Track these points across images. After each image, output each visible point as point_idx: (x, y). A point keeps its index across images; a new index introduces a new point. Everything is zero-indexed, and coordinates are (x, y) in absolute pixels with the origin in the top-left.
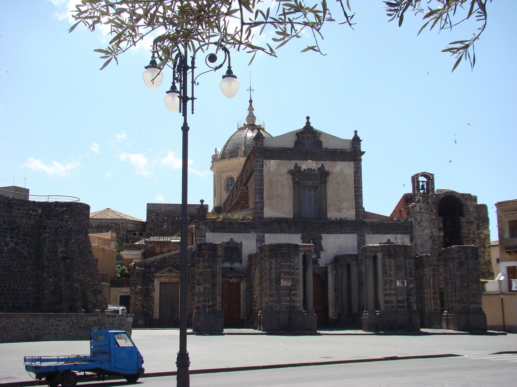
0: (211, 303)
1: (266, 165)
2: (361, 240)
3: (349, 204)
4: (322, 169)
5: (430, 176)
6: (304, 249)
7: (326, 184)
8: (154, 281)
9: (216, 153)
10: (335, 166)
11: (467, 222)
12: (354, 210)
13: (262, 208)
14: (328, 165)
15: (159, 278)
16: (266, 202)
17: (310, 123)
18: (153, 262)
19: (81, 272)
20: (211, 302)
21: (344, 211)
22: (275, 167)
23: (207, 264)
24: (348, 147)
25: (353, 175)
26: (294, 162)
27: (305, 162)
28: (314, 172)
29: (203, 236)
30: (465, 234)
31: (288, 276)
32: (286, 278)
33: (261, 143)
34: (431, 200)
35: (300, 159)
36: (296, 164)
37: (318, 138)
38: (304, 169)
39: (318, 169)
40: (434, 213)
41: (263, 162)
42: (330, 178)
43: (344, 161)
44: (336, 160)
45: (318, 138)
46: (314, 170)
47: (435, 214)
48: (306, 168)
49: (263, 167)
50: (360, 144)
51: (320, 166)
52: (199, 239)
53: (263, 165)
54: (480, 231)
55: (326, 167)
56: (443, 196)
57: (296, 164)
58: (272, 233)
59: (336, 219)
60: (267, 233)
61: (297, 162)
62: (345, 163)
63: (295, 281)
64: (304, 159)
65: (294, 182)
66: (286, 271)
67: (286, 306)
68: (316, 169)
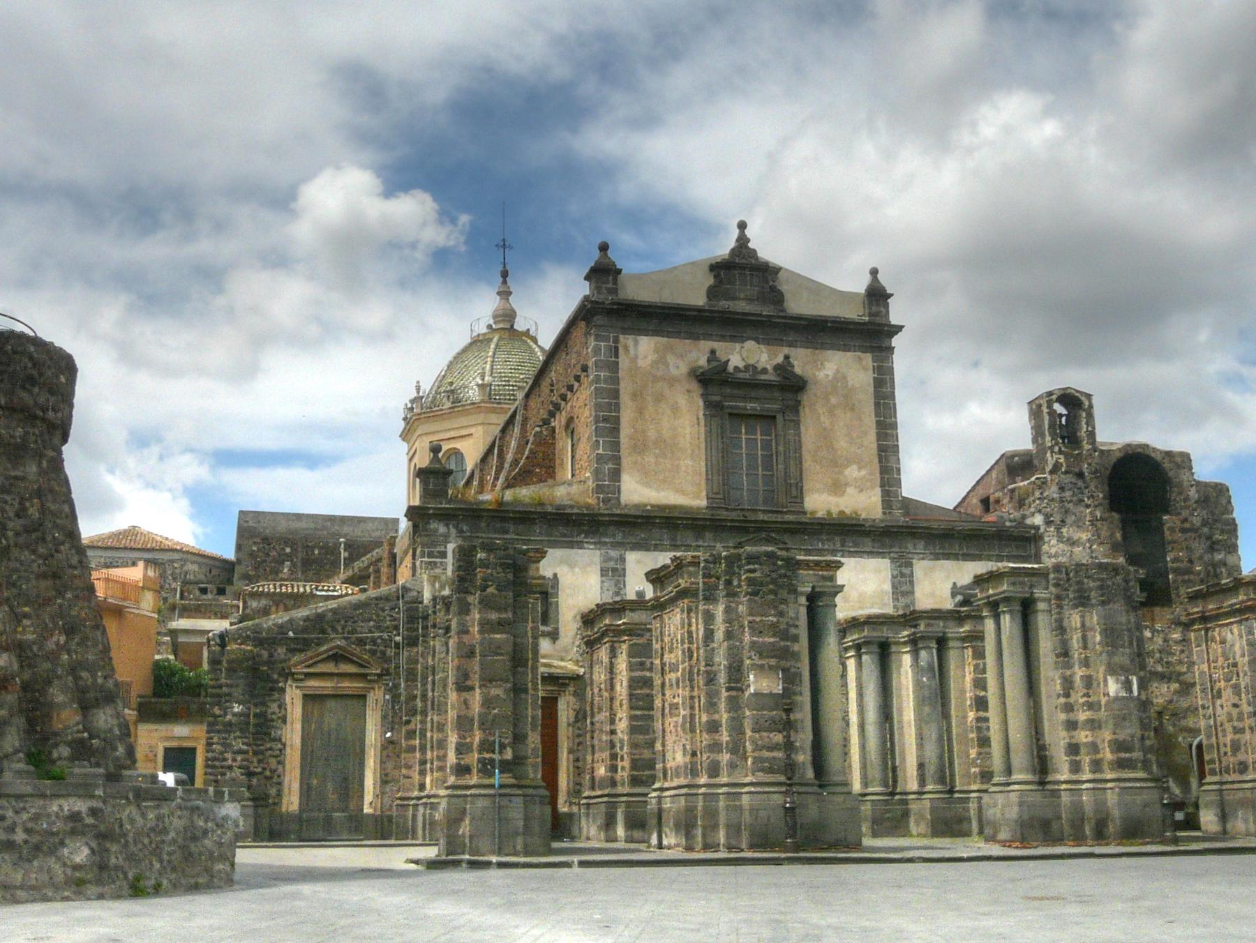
0: (508, 754)
1: (626, 348)
2: (903, 575)
3: (863, 473)
4: (784, 369)
5: (1083, 398)
6: (811, 572)
7: (797, 412)
8: (283, 690)
9: (418, 392)
10: (822, 364)
11: (1183, 531)
12: (878, 491)
13: (616, 475)
14: (802, 360)
15: (301, 680)
16: (626, 461)
17: (748, 241)
18: (282, 628)
19: (27, 609)
20: (508, 749)
21: (850, 490)
22: (652, 357)
23: (494, 616)
24: (853, 313)
25: (872, 389)
26: (706, 345)
27: (738, 346)
28: (763, 377)
29: (439, 552)
30: (1182, 561)
31: (773, 662)
32: (766, 666)
33: (610, 285)
34: (1089, 464)
35: (722, 338)
36: (713, 352)
37: (771, 283)
38: (736, 368)
39: (777, 368)
40: (1096, 503)
41: (616, 340)
42: (806, 398)
43: (846, 349)
44: (823, 347)
45: (771, 283)
46: (764, 371)
47: (1100, 504)
48: (741, 365)
49: (617, 356)
50: (887, 306)
51: (780, 359)
52: (426, 563)
53: (617, 349)
54: (1219, 557)
55: (796, 363)
56: (1119, 455)
57: (713, 352)
58: (648, 550)
59: (829, 513)
60: (632, 549)
61: (715, 345)
62: (849, 354)
63: (791, 679)
64: (733, 339)
65: (709, 405)
66: (763, 643)
67: (766, 764)
68: (769, 368)
